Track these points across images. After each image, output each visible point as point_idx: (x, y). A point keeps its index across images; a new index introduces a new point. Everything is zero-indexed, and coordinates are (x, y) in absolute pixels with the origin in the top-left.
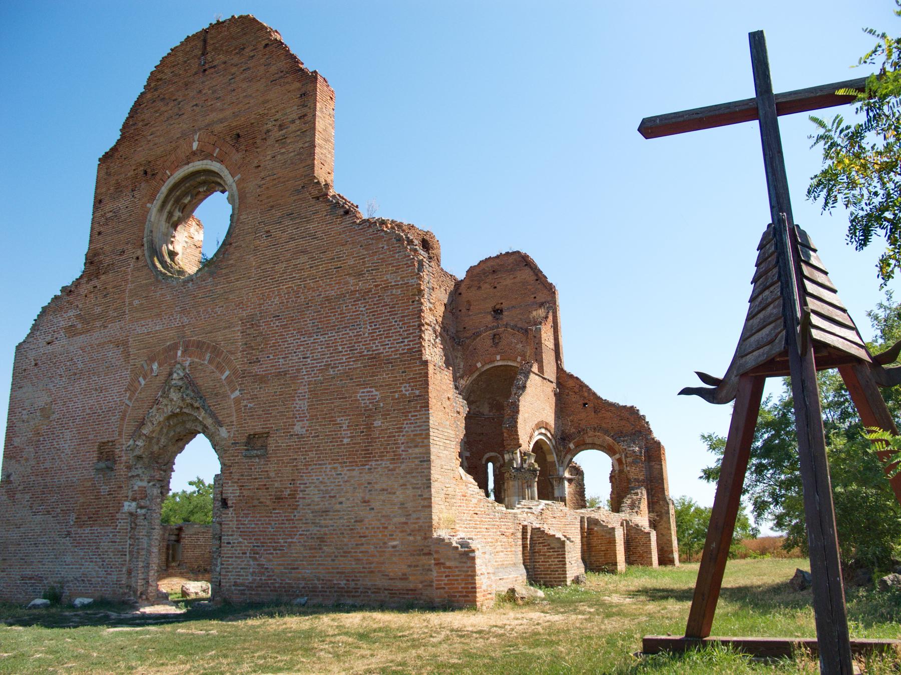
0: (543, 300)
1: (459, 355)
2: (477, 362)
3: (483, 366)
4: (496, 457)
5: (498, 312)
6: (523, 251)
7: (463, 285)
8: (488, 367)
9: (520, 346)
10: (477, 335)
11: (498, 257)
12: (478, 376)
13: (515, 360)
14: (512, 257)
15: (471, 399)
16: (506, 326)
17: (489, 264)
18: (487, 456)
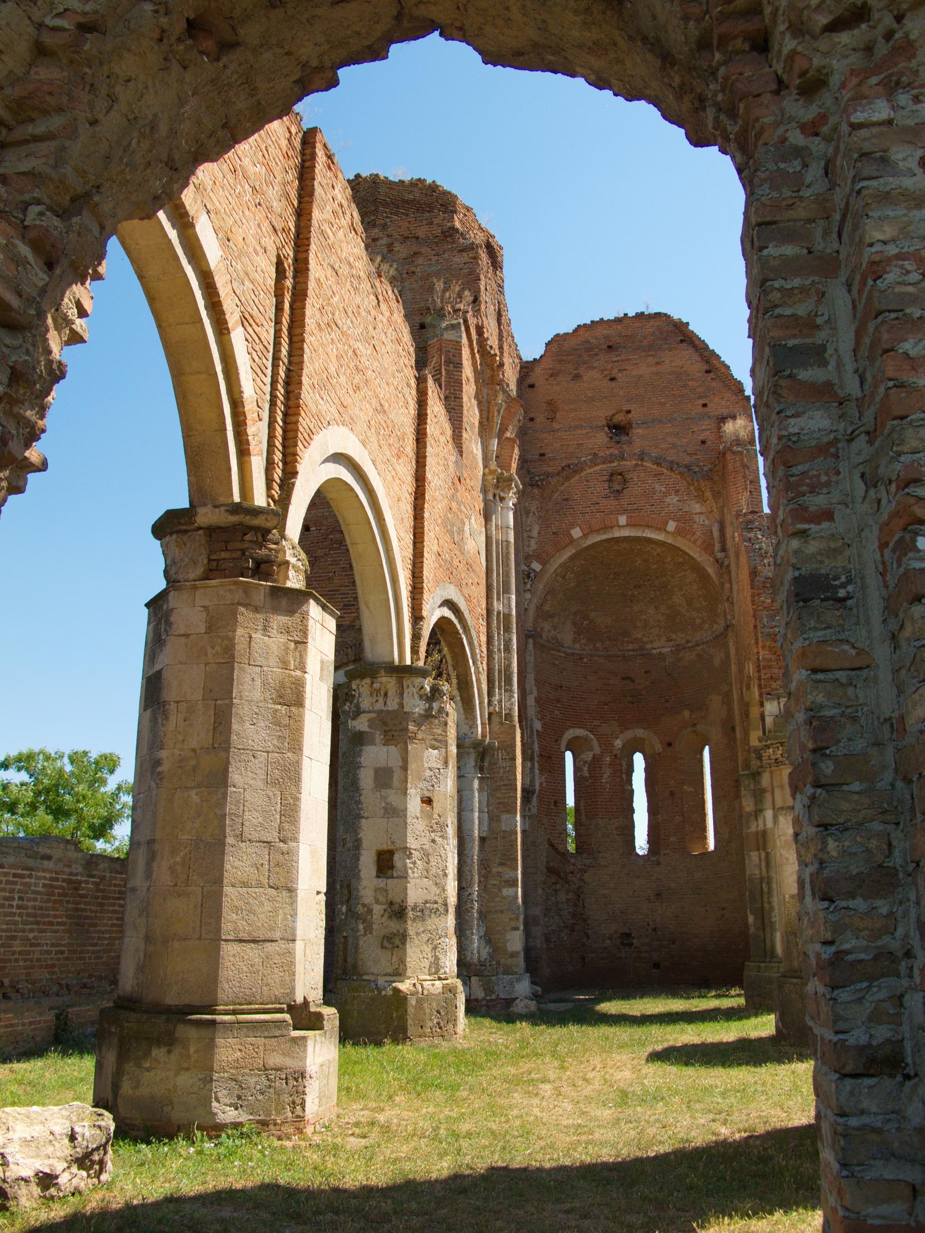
0: (725, 412)
1: (533, 509)
2: (572, 526)
3: (585, 536)
4: (586, 739)
5: (619, 430)
6: (676, 316)
7: (538, 370)
8: (591, 540)
9: (673, 499)
10: (571, 470)
11: (618, 320)
12: (572, 558)
13: (662, 528)
14: (652, 322)
15: (547, 607)
16: (642, 456)
17: (600, 332)
18: (570, 733)
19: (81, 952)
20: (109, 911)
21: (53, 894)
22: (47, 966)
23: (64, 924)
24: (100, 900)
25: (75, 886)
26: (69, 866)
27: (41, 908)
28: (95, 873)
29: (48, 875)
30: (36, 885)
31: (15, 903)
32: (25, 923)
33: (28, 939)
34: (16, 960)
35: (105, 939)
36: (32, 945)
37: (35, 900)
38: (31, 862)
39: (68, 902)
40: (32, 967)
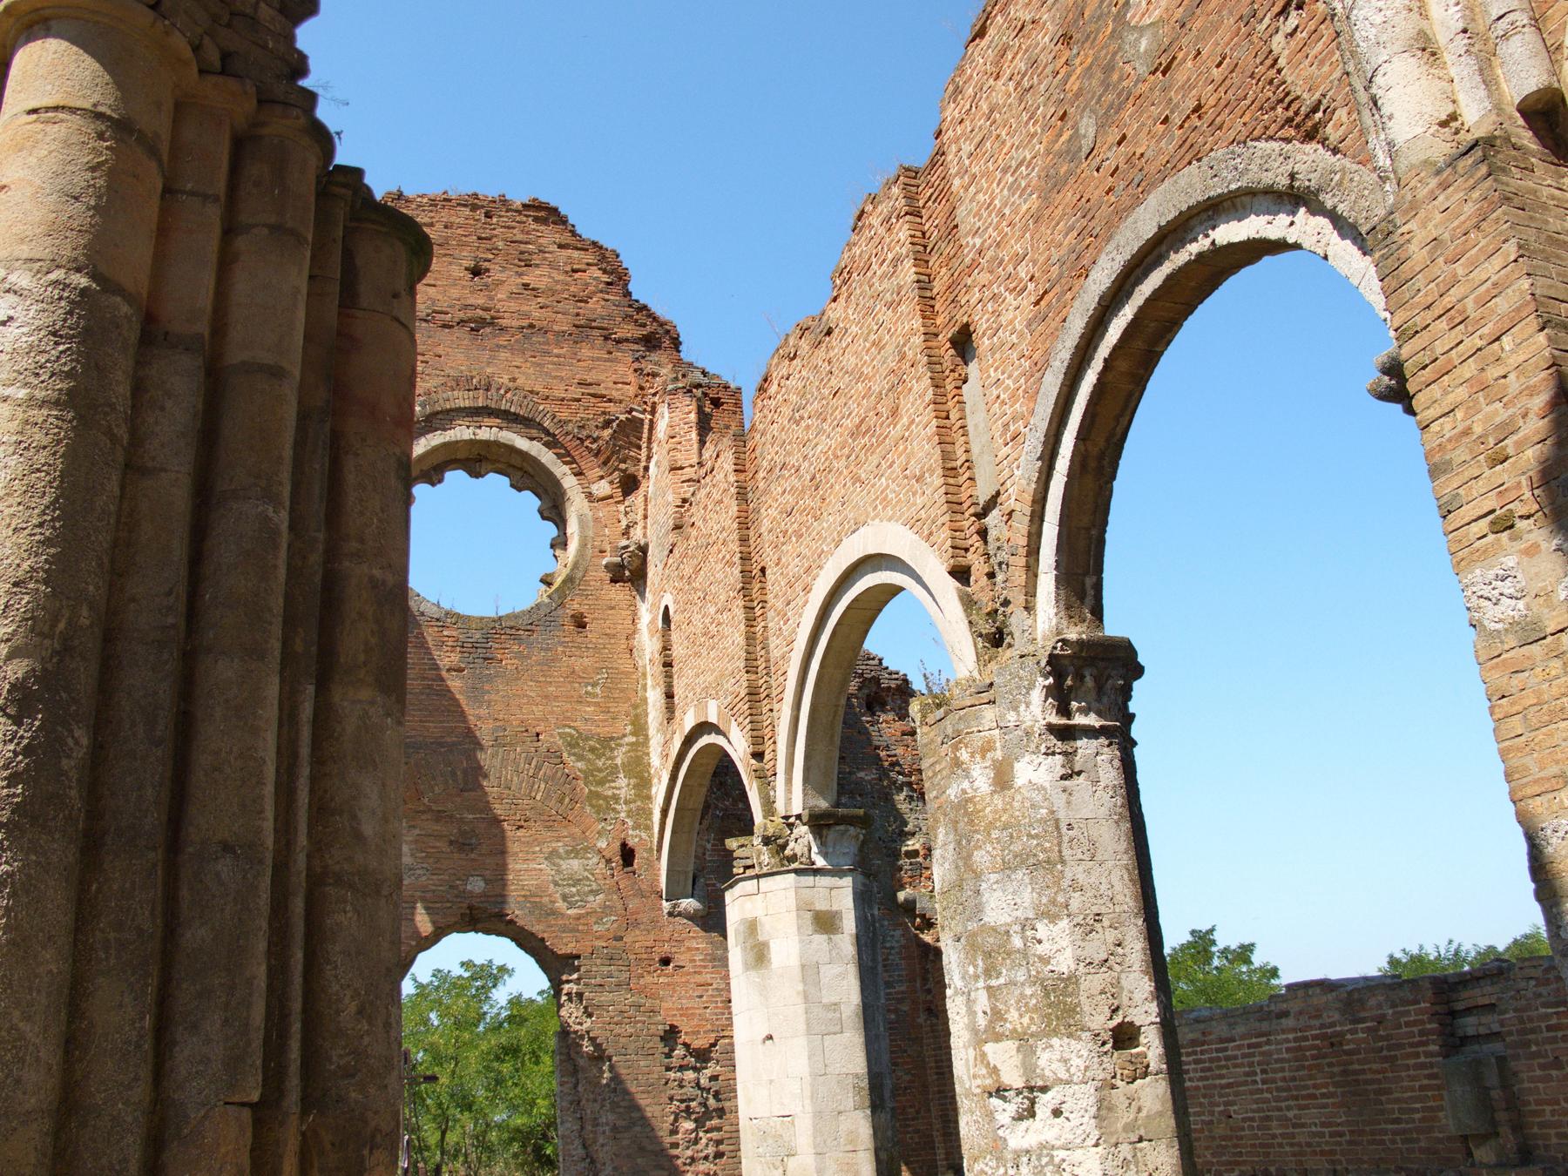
19: (1373, 1133)
20: (1408, 1067)
21: (1305, 1058)
22: (1323, 1153)
23: (1331, 1095)
24: (1385, 1053)
25: (1334, 1041)
26: (1318, 1017)
27: (1294, 1079)
28: (1363, 1014)
29: (1291, 1036)
30: (1279, 1051)
31: (1258, 1078)
32: (1277, 1099)
33: (1287, 1119)
34: (1281, 1145)
35: (1416, 1111)
36: (1295, 1126)
37: (1282, 1069)
38: (1265, 1026)
39: (1330, 1065)
40: (1301, 1154)
